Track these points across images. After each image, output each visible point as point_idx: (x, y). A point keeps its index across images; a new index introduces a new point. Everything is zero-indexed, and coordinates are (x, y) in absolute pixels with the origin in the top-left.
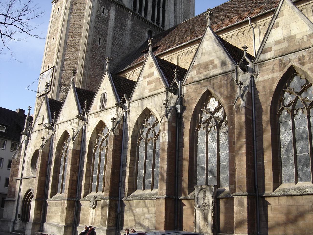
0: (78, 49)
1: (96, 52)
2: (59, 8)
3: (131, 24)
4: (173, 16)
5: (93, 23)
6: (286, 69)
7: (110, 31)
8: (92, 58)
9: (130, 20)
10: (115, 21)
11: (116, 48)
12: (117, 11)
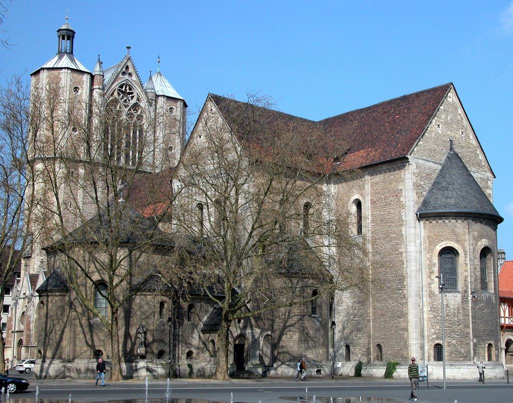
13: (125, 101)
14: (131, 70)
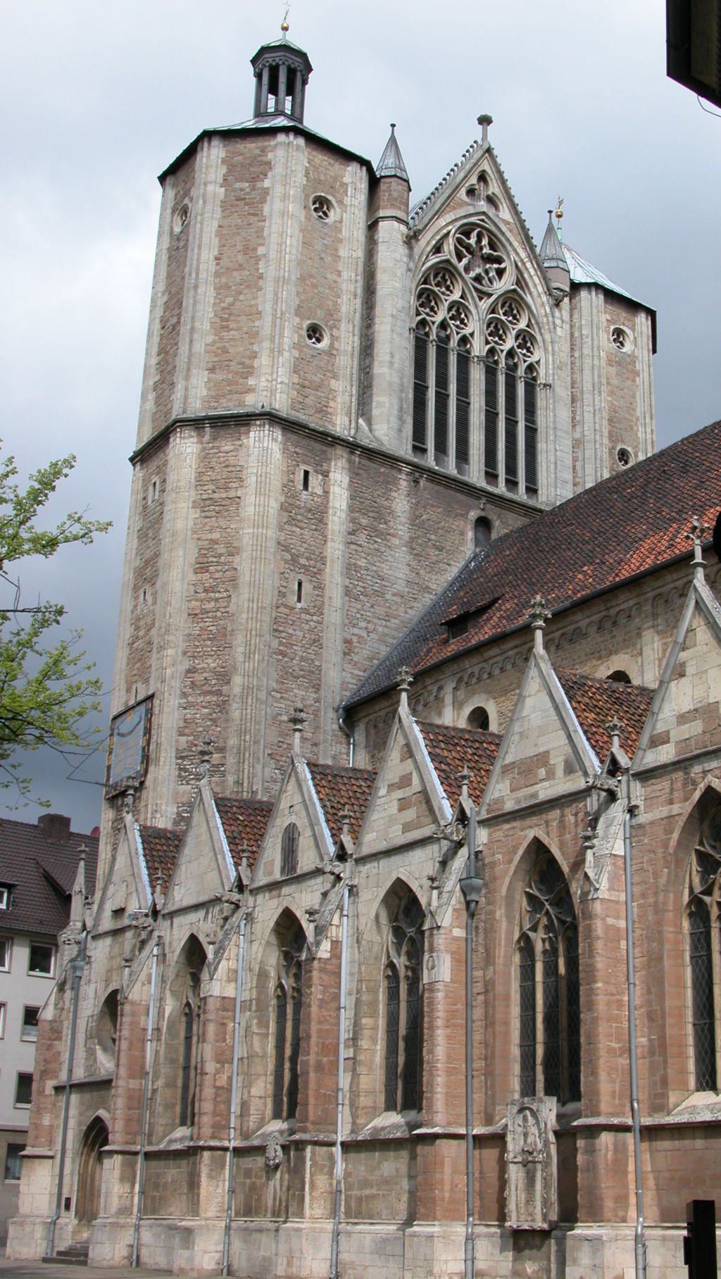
0: (229, 629)
1: (291, 631)
2: (155, 484)
3: (407, 507)
4: (566, 444)
5: (272, 533)
6: (697, 795)
7: (335, 549)
8: (276, 653)
9: (405, 493)
10: (351, 509)
11: (359, 607)
12: (354, 473)
13: (478, 279)
14: (494, 188)
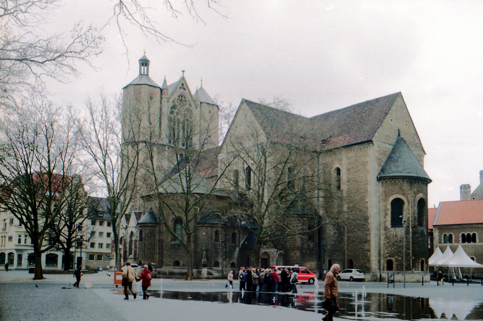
14: (185, 86)
